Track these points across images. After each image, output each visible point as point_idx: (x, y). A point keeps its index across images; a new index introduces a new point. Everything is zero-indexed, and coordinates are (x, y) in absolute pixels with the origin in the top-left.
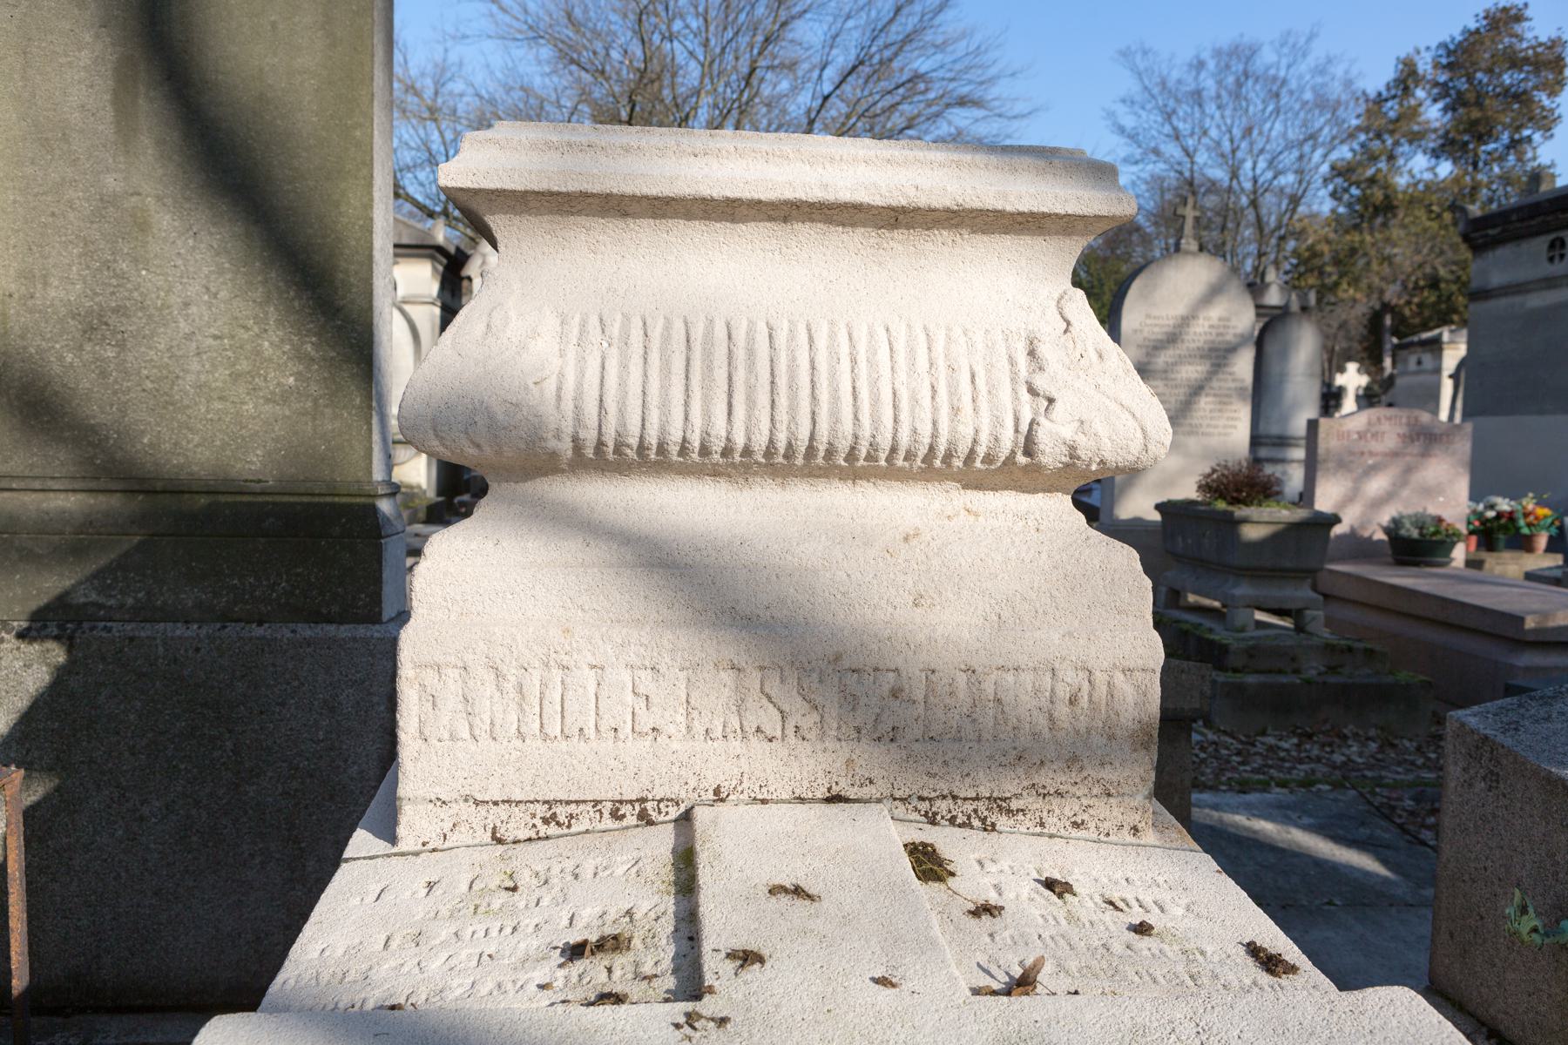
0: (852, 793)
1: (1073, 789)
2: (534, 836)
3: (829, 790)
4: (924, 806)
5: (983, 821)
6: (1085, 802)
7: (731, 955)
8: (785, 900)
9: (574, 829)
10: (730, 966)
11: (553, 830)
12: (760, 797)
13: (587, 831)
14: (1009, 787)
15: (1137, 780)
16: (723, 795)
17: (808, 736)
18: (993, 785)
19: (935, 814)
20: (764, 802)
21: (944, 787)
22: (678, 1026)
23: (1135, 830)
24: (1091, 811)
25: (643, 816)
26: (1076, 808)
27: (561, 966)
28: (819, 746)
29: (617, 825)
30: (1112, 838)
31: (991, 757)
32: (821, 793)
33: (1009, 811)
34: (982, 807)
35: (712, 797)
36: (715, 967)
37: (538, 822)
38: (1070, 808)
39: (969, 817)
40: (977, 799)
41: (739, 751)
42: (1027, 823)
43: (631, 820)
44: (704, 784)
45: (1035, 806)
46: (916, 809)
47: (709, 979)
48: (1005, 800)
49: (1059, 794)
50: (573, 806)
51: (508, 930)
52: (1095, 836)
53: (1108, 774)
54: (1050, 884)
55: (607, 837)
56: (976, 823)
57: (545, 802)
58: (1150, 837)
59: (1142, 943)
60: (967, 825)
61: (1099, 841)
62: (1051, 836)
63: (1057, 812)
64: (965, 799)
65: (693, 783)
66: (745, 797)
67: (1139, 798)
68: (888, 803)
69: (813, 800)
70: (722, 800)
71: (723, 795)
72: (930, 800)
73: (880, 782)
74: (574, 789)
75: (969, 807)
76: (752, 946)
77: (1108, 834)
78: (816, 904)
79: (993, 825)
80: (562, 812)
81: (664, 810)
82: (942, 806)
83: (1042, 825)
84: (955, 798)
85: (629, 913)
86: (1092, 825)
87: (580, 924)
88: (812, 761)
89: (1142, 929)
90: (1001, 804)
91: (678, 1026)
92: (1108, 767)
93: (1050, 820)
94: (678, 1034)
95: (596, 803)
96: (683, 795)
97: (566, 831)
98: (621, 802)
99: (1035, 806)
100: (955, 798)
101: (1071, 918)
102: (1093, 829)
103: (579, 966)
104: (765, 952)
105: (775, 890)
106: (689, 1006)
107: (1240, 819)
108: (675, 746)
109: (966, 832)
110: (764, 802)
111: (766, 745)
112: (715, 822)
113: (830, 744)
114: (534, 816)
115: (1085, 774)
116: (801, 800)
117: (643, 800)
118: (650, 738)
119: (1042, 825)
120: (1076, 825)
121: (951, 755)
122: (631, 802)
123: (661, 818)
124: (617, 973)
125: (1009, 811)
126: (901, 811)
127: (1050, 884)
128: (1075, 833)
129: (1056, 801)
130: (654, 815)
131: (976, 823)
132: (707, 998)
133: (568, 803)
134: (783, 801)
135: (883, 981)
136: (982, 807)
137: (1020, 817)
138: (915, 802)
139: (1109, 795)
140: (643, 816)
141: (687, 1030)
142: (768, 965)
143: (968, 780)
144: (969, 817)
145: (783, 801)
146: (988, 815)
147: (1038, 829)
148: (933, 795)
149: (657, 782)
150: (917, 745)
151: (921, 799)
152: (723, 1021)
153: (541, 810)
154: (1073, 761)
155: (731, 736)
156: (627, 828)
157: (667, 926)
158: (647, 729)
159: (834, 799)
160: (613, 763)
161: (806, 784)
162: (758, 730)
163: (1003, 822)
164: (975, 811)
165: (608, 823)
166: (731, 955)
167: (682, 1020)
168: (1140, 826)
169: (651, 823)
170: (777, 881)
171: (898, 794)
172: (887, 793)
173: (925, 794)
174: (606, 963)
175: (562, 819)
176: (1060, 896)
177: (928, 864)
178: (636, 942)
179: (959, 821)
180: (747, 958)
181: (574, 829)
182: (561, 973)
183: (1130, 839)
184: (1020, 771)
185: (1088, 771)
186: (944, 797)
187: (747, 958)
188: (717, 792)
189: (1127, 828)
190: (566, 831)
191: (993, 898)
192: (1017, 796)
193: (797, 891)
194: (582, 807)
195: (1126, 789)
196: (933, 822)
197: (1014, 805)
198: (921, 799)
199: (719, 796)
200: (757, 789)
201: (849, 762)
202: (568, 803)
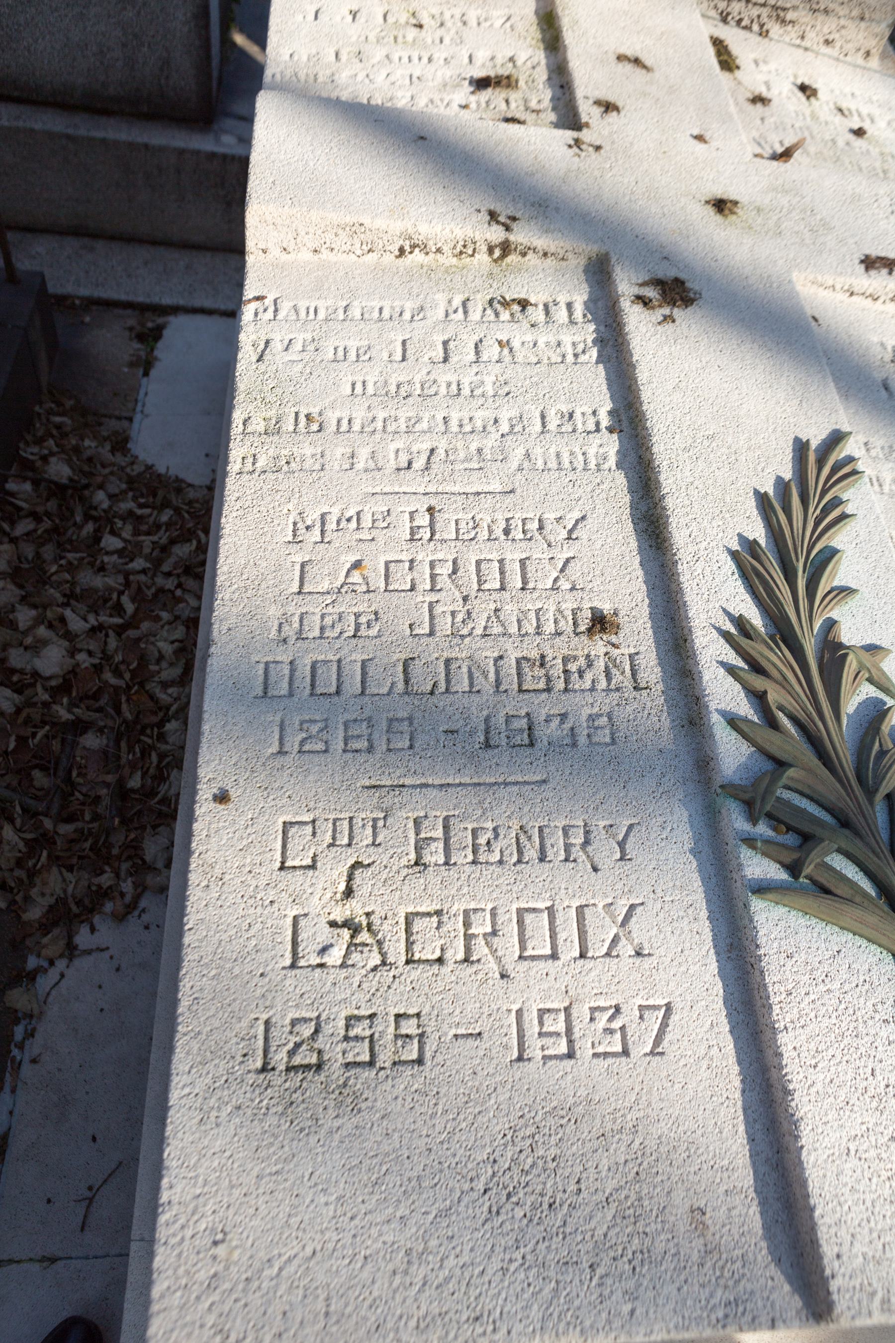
6: (843, 22)
7: (598, 103)
8: (629, 67)
19: (728, 14)
22: (570, 146)
23: (868, 54)
24: (843, 32)
26: (834, 26)
30: (848, 58)
36: (587, 111)
38: (827, 25)
39: (752, 22)
42: (792, 33)
45: (805, 20)
46: (715, 7)
47: (584, 118)
48: (784, 9)
49: (826, 11)
51: (425, 60)
54: (803, 88)
56: (756, 27)
58: (874, 62)
59: (858, 143)
60: (748, 28)
62: (806, 49)
63: (818, 28)
76: (611, 98)
78: (650, 74)
79: (767, 31)
85: (511, 59)
86: (838, 45)
89: (859, 132)
91: (570, 146)
93: (811, 35)
99: (805, 20)
101: (814, 116)
103: (486, 94)
104: (620, 104)
105: (621, 58)
106: (575, 134)
119: (803, 37)
120: (827, 42)
124: (513, 105)
127: (803, 88)
128: (824, 50)
129: (821, 17)
132: (585, 131)
135: (700, 138)
136: (765, 12)
137: (789, 28)
141: (575, 149)
142: (622, 113)
147: (798, 42)
152: (598, 148)
157: (542, 75)
163: (775, 30)
164: (759, 16)
166: (598, 103)
167: (572, 143)
176: (808, 98)
178: (521, 83)
179: (743, 24)
180: (609, 107)
182: (473, 99)
183: (860, 61)
187: (609, 107)
189: (862, 51)
191: (765, 94)
192: (795, 8)
193: (637, 61)
196: (724, 20)
197: (790, 16)
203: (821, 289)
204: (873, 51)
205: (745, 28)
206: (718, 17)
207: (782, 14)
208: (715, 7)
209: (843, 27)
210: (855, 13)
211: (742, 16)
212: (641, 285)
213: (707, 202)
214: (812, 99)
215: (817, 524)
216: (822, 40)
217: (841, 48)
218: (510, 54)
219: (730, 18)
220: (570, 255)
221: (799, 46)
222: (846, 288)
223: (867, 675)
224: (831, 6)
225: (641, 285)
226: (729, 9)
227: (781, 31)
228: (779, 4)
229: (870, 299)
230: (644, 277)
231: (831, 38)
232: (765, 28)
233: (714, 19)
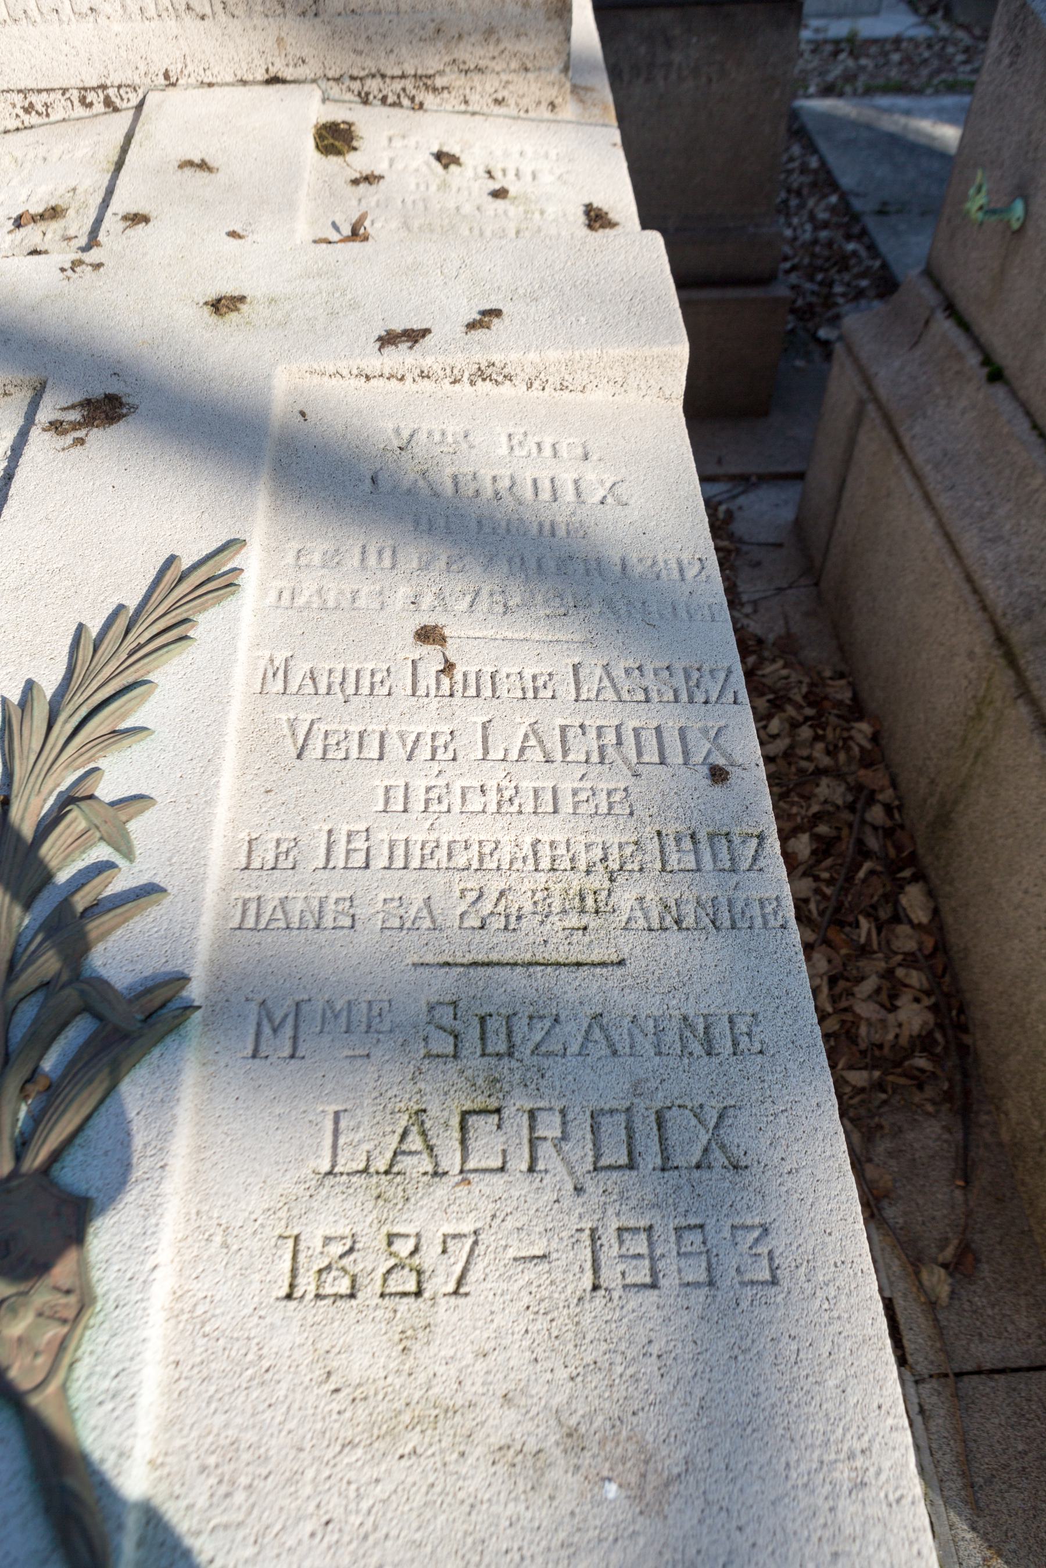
0: (288, 73)
1: (492, 64)
2: (20, 126)
3: (267, 70)
4: (356, 85)
5: (412, 99)
6: (504, 77)
8: (188, 172)
9: (52, 118)
10: (123, 225)
11: (34, 119)
12: (206, 80)
13: (64, 120)
14: (432, 63)
15: (552, 52)
16: (173, 80)
17: (236, 13)
18: (416, 61)
19: (367, 94)
20: (210, 85)
21: (371, 65)
22: (63, 270)
23: (552, 106)
24: (511, 87)
25: (108, 102)
26: (496, 84)
27: (10, 232)
28: (249, 24)
29: (87, 112)
31: (411, 31)
32: (261, 75)
33: (435, 89)
34: (409, 84)
35: (163, 82)
37: (21, 113)
38: (490, 84)
39: (399, 97)
40: (403, 76)
41: (175, 32)
42: (452, 101)
43: (99, 107)
44: (153, 69)
45: (458, 83)
46: (349, 89)
48: (429, 77)
49: (479, 70)
50: (44, 94)
52: (515, 113)
53: (524, 47)
55: (79, 124)
56: (406, 102)
57: (20, 91)
59: (500, 204)
61: (519, 118)
62: (474, 114)
63: (479, 88)
64: (393, 78)
65: (143, 68)
66: (192, 80)
67: (555, 71)
68: (323, 84)
69: (254, 82)
70: (174, 85)
71: (173, 80)
72: (361, 79)
73: (312, 61)
74: (39, 76)
75: (397, 86)
77: (527, 111)
78: (213, 176)
79: (421, 105)
80: (38, 100)
81: (125, 96)
82: (373, 85)
83: (466, 102)
84: (383, 76)
86: (512, 102)
87: (33, 199)
88: (245, 41)
90: (425, 81)
91: (63, 270)
92: (523, 39)
93: (474, 98)
94: (62, 275)
95: (64, 91)
96: (137, 81)
97: (46, 120)
98: (85, 89)
99: (458, 83)
100: (383, 76)
102: (513, 106)
108: (116, 27)
109: (396, 111)
110: (210, 85)
111: (198, 22)
112: (159, 106)
113: (259, 21)
114: (14, 106)
115: (501, 47)
116: (244, 83)
117: (104, 87)
118: (91, 19)
119: (466, 102)
120: (498, 102)
121: (372, 30)
122: (93, 89)
123: (125, 105)
124: (49, 236)
125: (435, 89)
126: (335, 90)
127: (439, 156)
128: (497, 110)
129: (477, 77)
130: (117, 101)
131: (406, 102)
133: (40, 91)
134: (227, 84)
135: (233, 234)
136: (409, 84)
138: (347, 82)
139: (526, 70)
140: (108, 102)
141: (69, 273)
142: (151, 224)
143: (392, 57)
144: (399, 97)
145: (227, 84)
146: (413, 93)
147: (463, 107)
148: (362, 74)
149: (110, 67)
150: (340, 19)
151: (353, 78)
152: (99, 265)
153: (18, 99)
154: (489, 33)
155: (165, 14)
156: (96, 115)
158: (85, 9)
159: (274, 80)
160: (66, 49)
161: (245, 67)
162: (189, 7)
163: (430, 100)
164: (404, 90)
165: (80, 111)
166: (125, 218)
167: (67, 265)
168: (556, 102)
169: (116, 110)
170: (188, 157)
171: (330, 74)
172: (320, 73)
173: (355, 73)
174: (43, 228)
175: (39, 107)
176: (446, 167)
177: (334, 139)
178: (71, 213)
179: (390, 100)
181: (52, 118)
183: (548, 115)
184: (440, 45)
185: (505, 44)
186: (373, 76)
187: (137, 219)
188: (167, 76)
189: (544, 105)
190: (46, 120)
192: (442, 73)
193: (203, 166)
194: (52, 95)
195: (542, 63)
196: (365, 102)
197: (439, 82)
198: (353, 78)
199: (170, 81)
200: (202, 72)
201: (280, 40)
202: (40, 91)
203: (326, 378)
204: (558, 101)
205: (393, 105)
206: (357, 99)
207: (429, 82)
208: (349, 89)
209: (508, 82)
210: (514, 65)
211: (384, 93)
212: (63, 409)
213: (206, 303)
214: (453, 168)
215: (130, 655)
216: (490, 101)
217: (517, 105)
218: (73, 185)
219: (371, 97)
220: (10, 388)
221: (465, 112)
222: (355, 372)
223: (98, 835)
224: (482, 63)
225: (63, 409)
226: (366, 89)
227: (438, 100)
228: (419, 72)
229: (394, 381)
230: (78, 398)
231: (500, 97)
232: (417, 100)
233: (351, 102)
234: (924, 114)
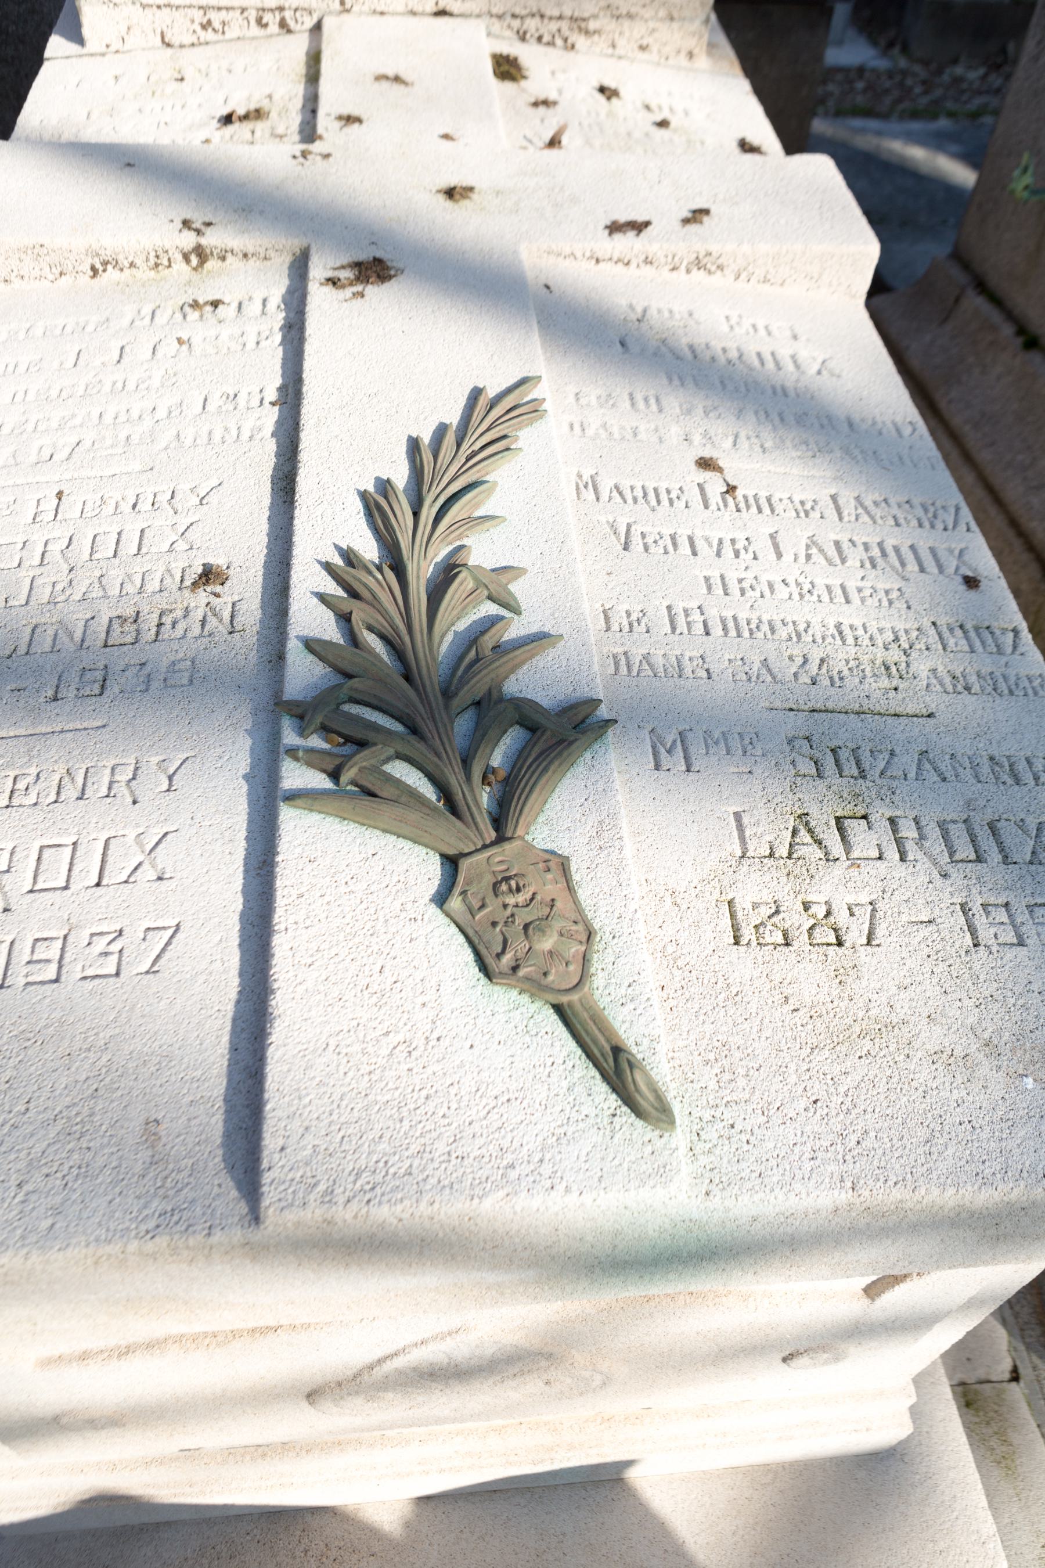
1: (643, 12)
2: (196, 41)
4: (516, 23)
5: (566, 40)
6: (652, 24)
7: (340, 118)
8: (385, 85)
10: (337, 124)
11: (209, 35)
12: (379, 9)
19: (525, 33)
20: (382, 13)
22: (294, 157)
23: (691, 55)
24: (656, 35)
25: (283, 24)
30: (671, 62)
32: (430, 7)
33: (587, 32)
34: (564, 25)
36: (324, 123)
37: (198, 29)
38: (637, 31)
39: (553, 37)
40: (560, 18)
42: (601, 44)
43: (273, 28)
46: (509, 26)
47: (320, 130)
48: (584, 20)
49: (630, 16)
50: (224, 12)
51: (178, 107)
54: (602, 90)
56: (559, 42)
57: (200, 8)
58: (703, 61)
59: (662, 132)
60: (551, 44)
62: (620, 57)
63: (627, 34)
64: (551, 18)
69: (423, 14)
70: (348, 11)
71: (348, 6)
72: (522, 18)
75: (554, 26)
76: (355, 113)
77: (667, 58)
79: (573, 47)
80: (216, 18)
81: (300, 20)
84: (542, 16)
85: (270, 97)
86: (655, 48)
89: (663, 124)
91: (294, 157)
93: (621, 43)
94: (294, 162)
95: (243, 10)
97: (220, 37)
98: (263, 10)
100: (542, 16)
101: (610, 114)
103: (230, 129)
104: (364, 117)
105: (380, 78)
106: (304, 147)
107: (917, 154)
110: (382, 13)
114: (193, 21)
116: (413, 13)
117: (281, 9)
119: (614, 46)
120: (643, 48)
122: (272, 10)
126: (497, 26)
127: (602, 90)
129: (626, 23)
130: (291, 24)
131: (559, 42)
132: (317, 143)
133: (219, 9)
135: (446, 137)
136: (564, 25)
137: (596, 37)
140: (283, 24)
141: (301, 160)
142: (364, 125)
147: (610, 51)
148: (524, 12)
152: (327, 156)
153: (198, 15)
156: (271, 36)
157: (298, 102)
159: (442, 13)
163: (581, 41)
164: (559, 31)
165: (255, 30)
166: (340, 118)
167: (298, 154)
169: (289, 31)
171: (494, 11)
172: (485, 9)
175: (217, 25)
176: (609, 98)
178: (273, 115)
179: (545, 39)
180: (350, 120)
181: (228, 36)
182: (218, 134)
186: (533, 15)
187: (350, 120)
191: (553, 96)
192: (595, 17)
193: (397, 79)
194: (231, 13)
197: (592, 25)
202: (219, 9)
203: (561, 259)
204: (696, 51)
205: (548, 44)
206: (515, 37)
207: (583, 25)
208: (509, 26)
209: (654, 30)
210: (662, 13)
211: (541, 32)
212: (335, 269)
213: (439, 191)
214: (614, 100)
215: (468, 460)
216: (636, 46)
217: (659, 51)
218: (268, 92)
219: (528, 36)
220: (271, 253)
221: (612, 56)
222: (588, 254)
223: (486, 593)
224: (633, 10)
225: (335, 269)
226: (525, 27)
227: (589, 42)
228: (576, 14)
229: (620, 264)
230: (345, 260)
231: (645, 42)
232: (570, 41)
233: (509, 38)
234: (895, 136)
